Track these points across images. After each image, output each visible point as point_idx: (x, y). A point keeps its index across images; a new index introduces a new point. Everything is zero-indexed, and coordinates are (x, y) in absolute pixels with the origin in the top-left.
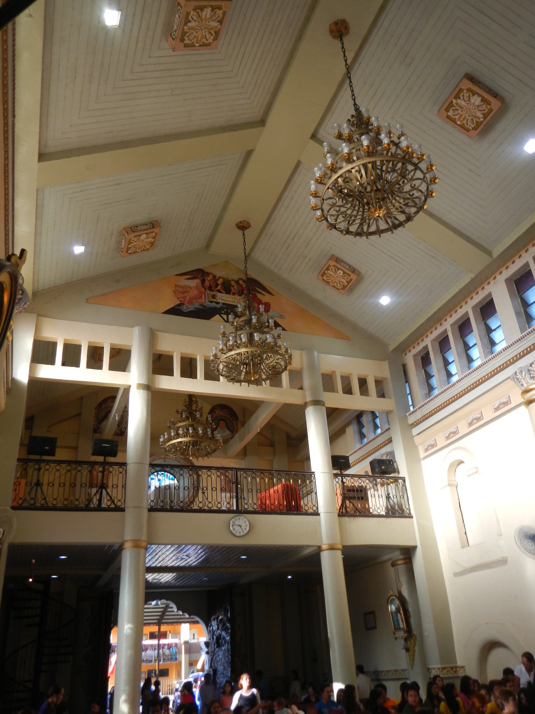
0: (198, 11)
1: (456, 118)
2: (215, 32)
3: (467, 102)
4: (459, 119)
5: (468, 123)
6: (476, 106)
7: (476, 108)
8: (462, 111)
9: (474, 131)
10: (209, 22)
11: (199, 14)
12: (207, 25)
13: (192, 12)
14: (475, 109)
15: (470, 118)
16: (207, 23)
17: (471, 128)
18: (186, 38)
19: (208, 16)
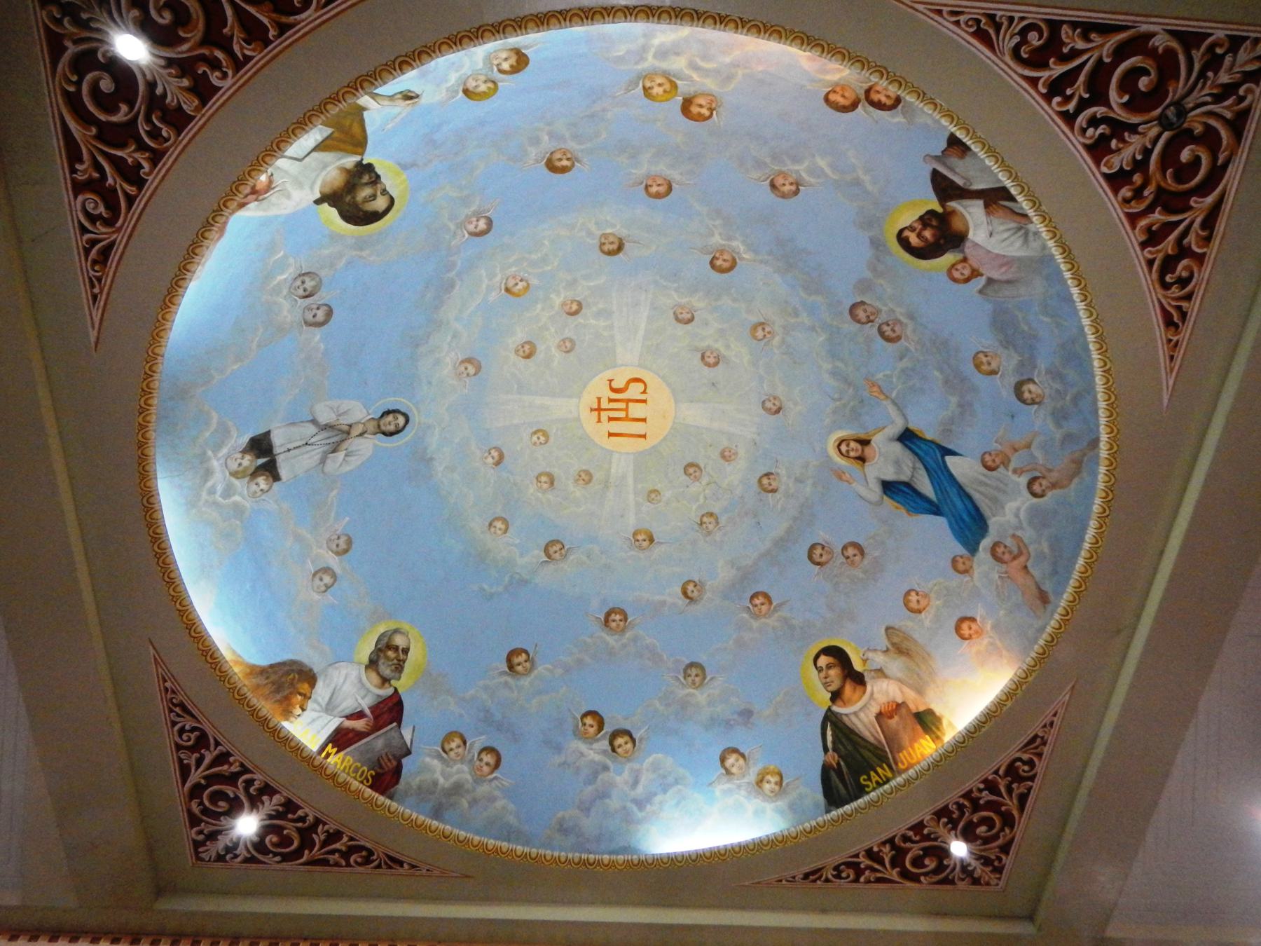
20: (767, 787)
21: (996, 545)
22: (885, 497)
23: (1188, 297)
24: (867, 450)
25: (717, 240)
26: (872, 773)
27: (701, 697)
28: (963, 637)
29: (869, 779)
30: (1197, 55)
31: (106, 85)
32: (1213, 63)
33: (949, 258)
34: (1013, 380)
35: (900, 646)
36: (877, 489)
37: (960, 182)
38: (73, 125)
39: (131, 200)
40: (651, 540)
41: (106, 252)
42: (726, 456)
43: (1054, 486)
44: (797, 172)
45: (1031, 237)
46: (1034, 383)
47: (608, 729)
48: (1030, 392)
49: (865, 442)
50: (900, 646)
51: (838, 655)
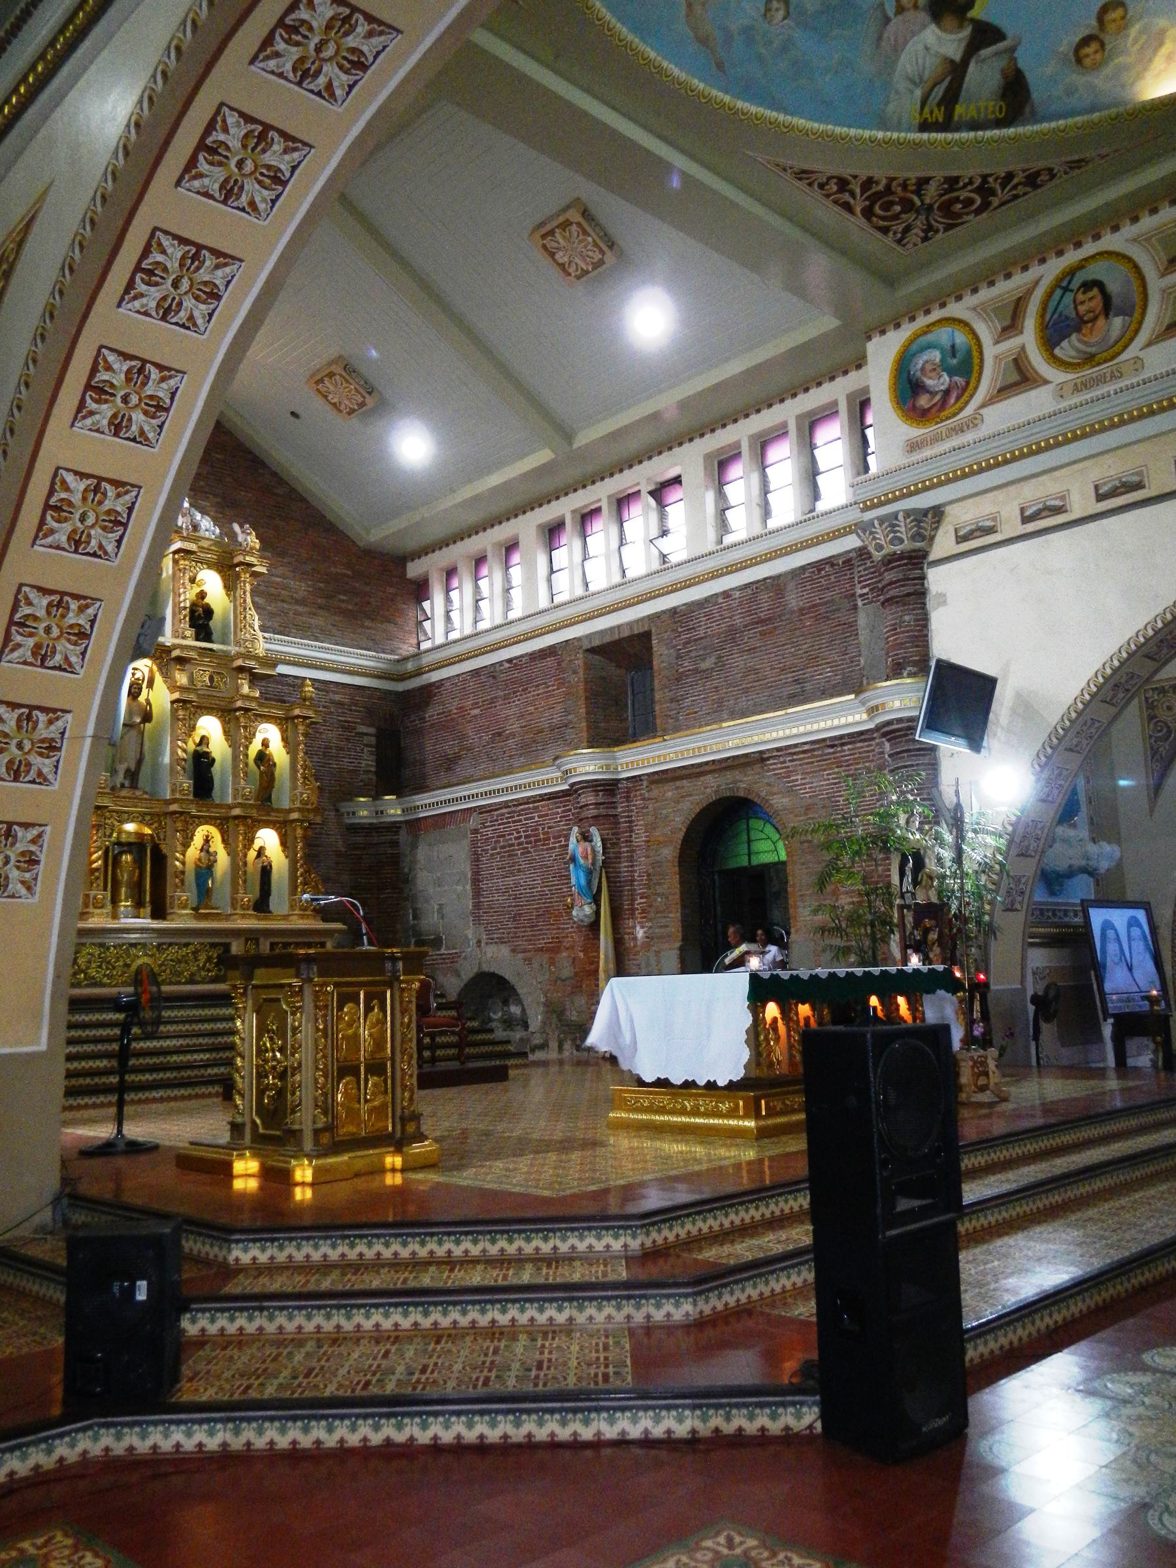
23: (810, 185)
30: (941, 227)
37: (985, 52)
45: (911, 86)
46: (784, 18)
48: (777, 10)
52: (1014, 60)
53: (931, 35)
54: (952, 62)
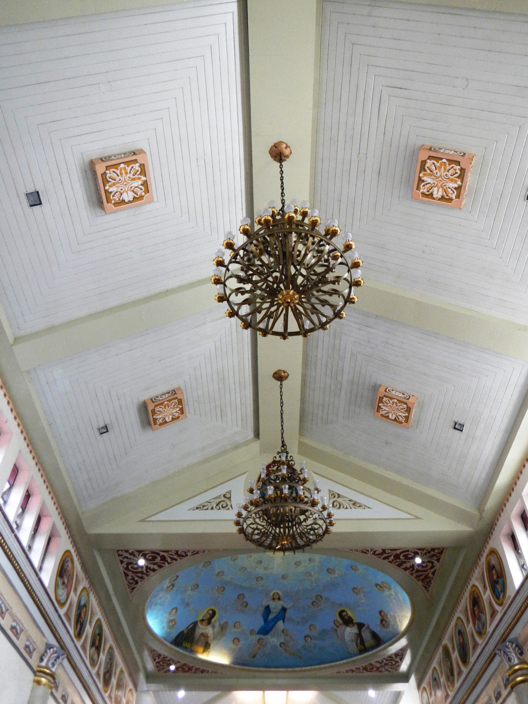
0: (447, 197)
1: (128, 166)
2: (425, 170)
3: (133, 188)
4: (125, 169)
5: (114, 173)
6: (124, 192)
7: (122, 191)
8: (129, 177)
9: (103, 172)
10: (434, 183)
11: (446, 193)
12: (435, 180)
13: (454, 197)
14: (122, 189)
15: (117, 180)
16: (436, 183)
17: (108, 172)
18: (459, 172)
19: (435, 189)
20: (171, 624)
21: (262, 639)
22: (264, 608)
24: (277, 600)
25: (337, 572)
26: (187, 643)
27: (189, 592)
28: (233, 641)
29: (185, 643)
31: (410, 556)
32: (392, 668)
33: (341, 621)
34: (309, 634)
35: (223, 628)
36: (265, 604)
37: (363, 629)
38: (401, 551)
39: (380, 558)
40: (235, 560)
41: (366, 553)
42: (265, 568)
43: (285, 649)
44: (360, 595)
47: (173, 582)
49: (279, 599)
50: (223, 628)
51: (214, 613)
52: (370, 629)
53: (348, 629)
54: (356, 634)
